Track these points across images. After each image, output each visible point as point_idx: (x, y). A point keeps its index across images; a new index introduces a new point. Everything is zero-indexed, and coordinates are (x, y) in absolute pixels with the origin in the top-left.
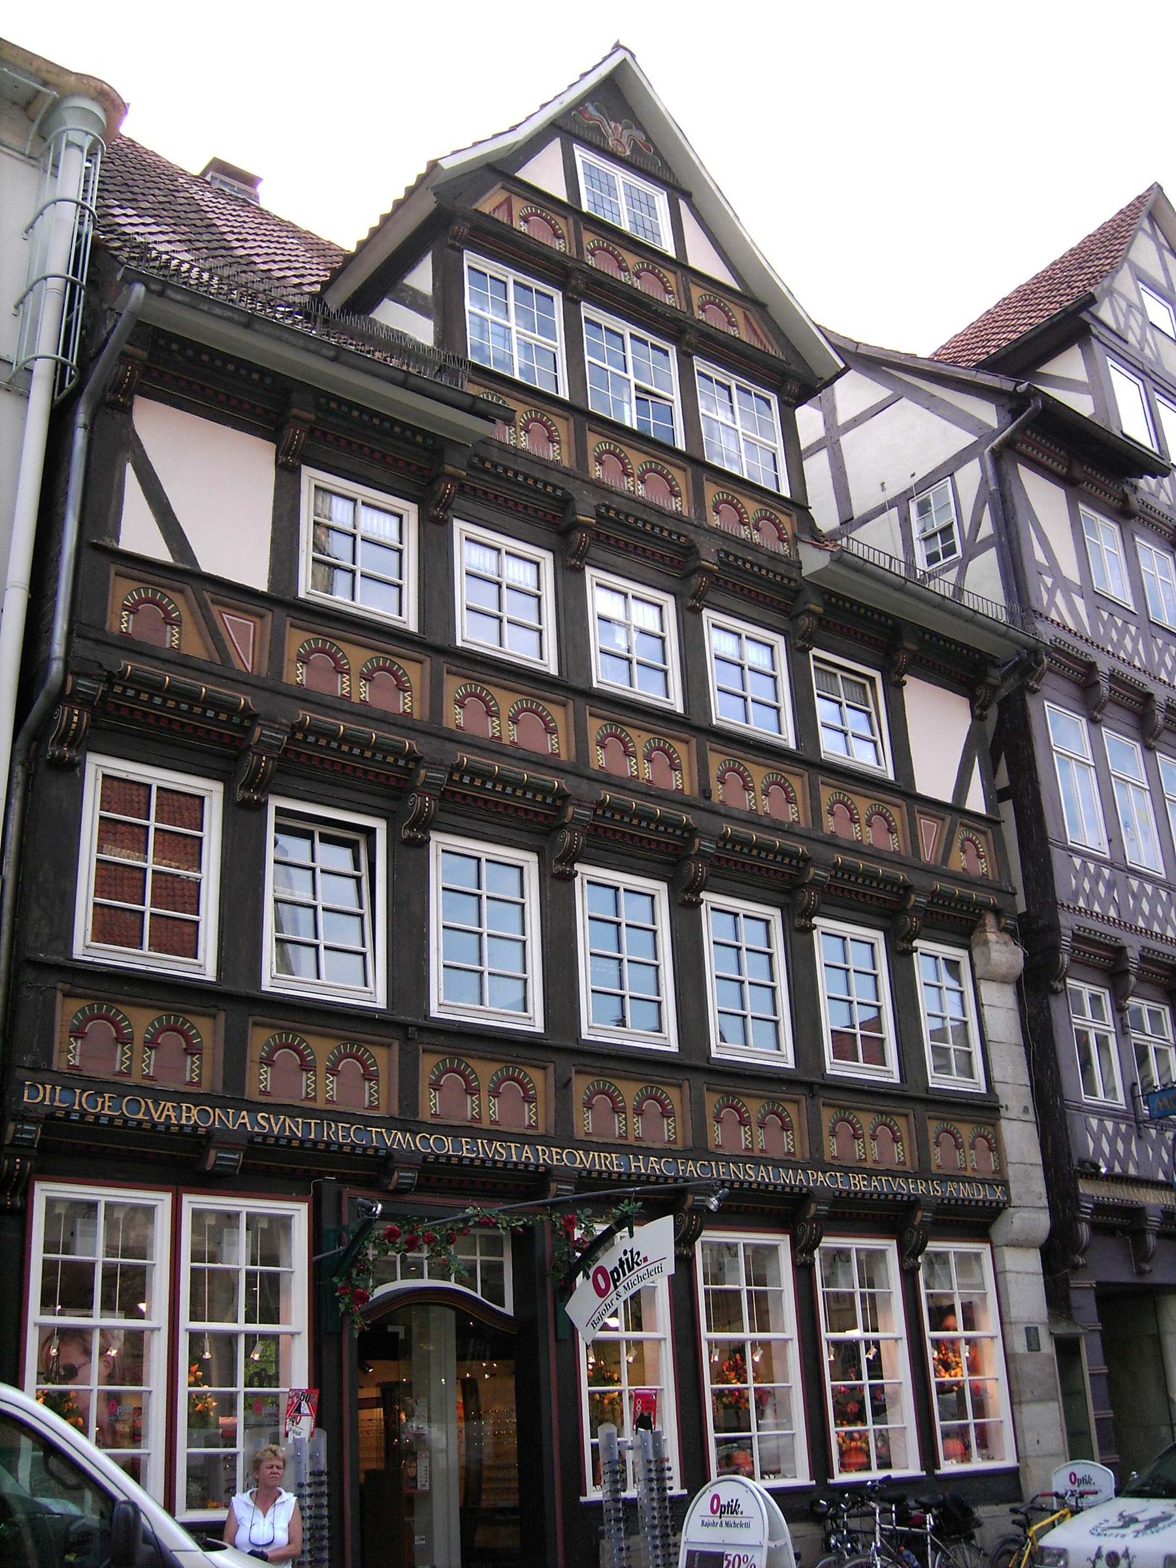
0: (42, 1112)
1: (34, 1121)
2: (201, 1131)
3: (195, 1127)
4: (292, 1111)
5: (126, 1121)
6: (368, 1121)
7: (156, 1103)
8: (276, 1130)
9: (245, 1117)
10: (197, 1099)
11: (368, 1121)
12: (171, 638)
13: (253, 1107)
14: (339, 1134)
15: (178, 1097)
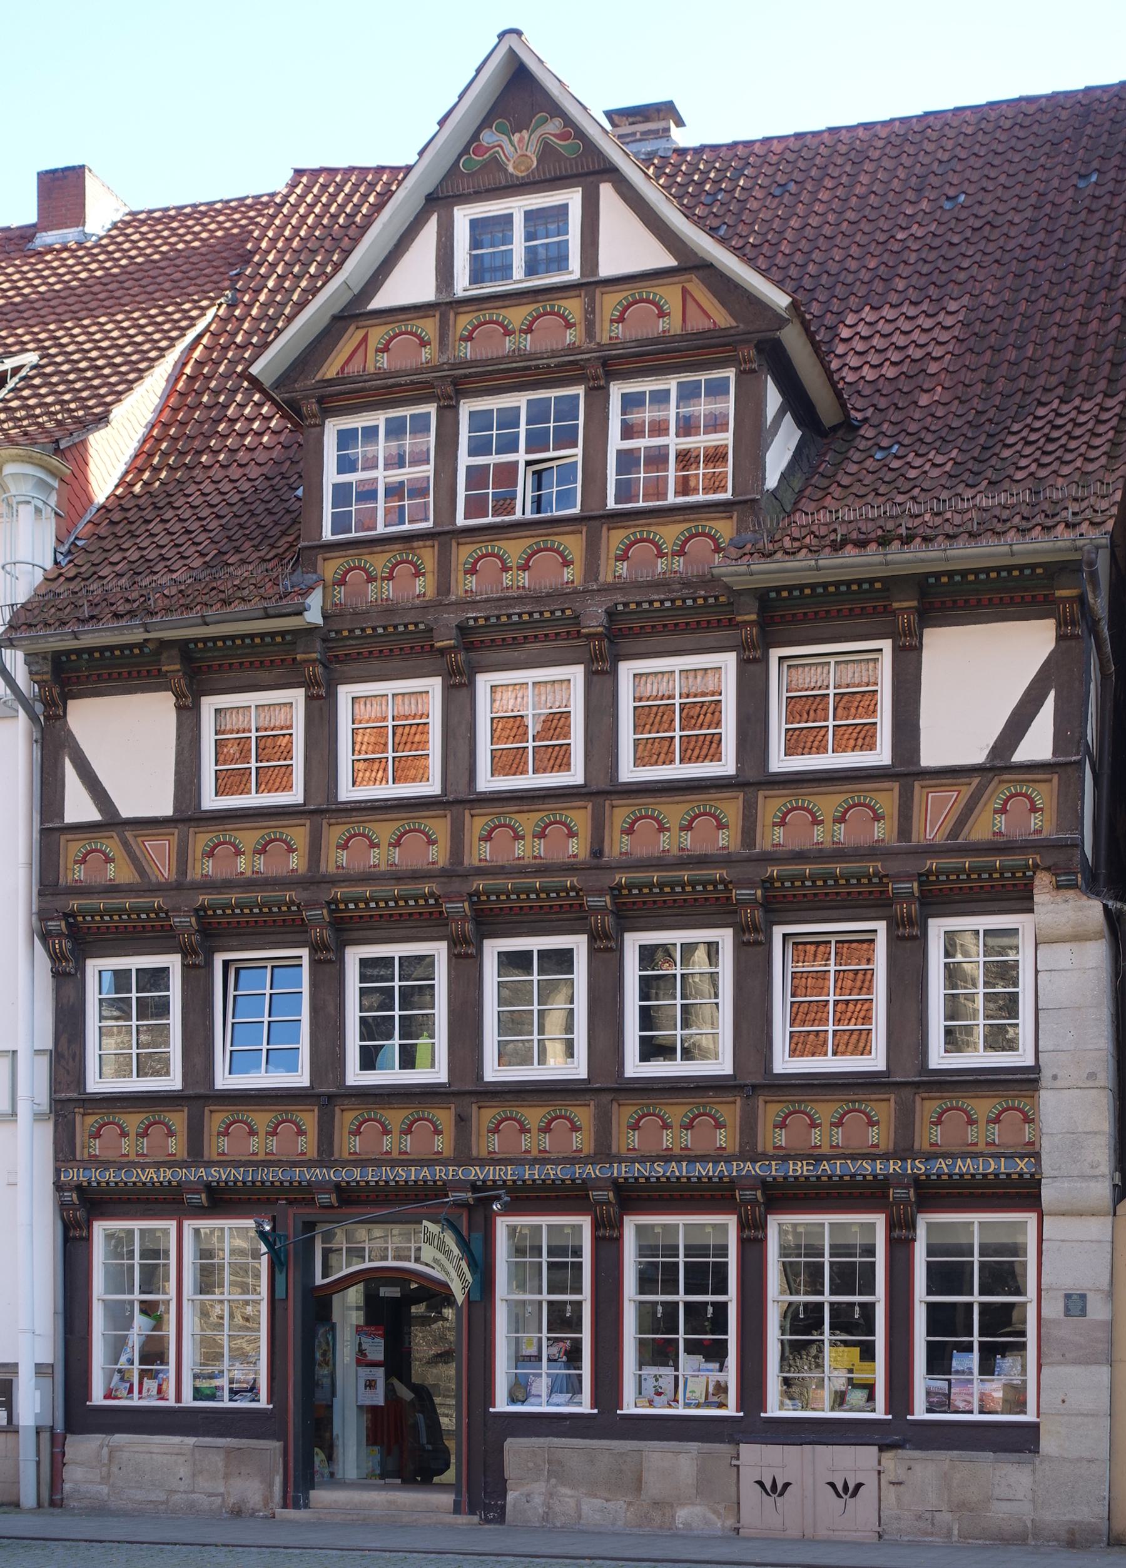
0: (73, 1184)
1: (70, 1190)
2: (174, 1184)
3: (170, 1182)
4: (237, 1164)
5: (126, 1183)
6: (294, 1164)
7: (143, 1169)
8: (224, 1177)
9: (202, 1172)
10: (170, 1165)
11: (294, 1164)
12: (111, 870)
13: (210, 1164)
14: (271, 1175)
15: (158, 1165)
